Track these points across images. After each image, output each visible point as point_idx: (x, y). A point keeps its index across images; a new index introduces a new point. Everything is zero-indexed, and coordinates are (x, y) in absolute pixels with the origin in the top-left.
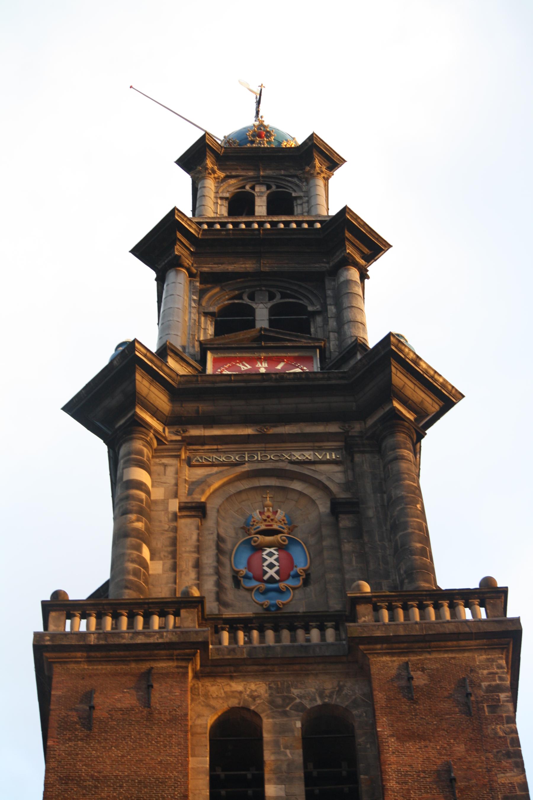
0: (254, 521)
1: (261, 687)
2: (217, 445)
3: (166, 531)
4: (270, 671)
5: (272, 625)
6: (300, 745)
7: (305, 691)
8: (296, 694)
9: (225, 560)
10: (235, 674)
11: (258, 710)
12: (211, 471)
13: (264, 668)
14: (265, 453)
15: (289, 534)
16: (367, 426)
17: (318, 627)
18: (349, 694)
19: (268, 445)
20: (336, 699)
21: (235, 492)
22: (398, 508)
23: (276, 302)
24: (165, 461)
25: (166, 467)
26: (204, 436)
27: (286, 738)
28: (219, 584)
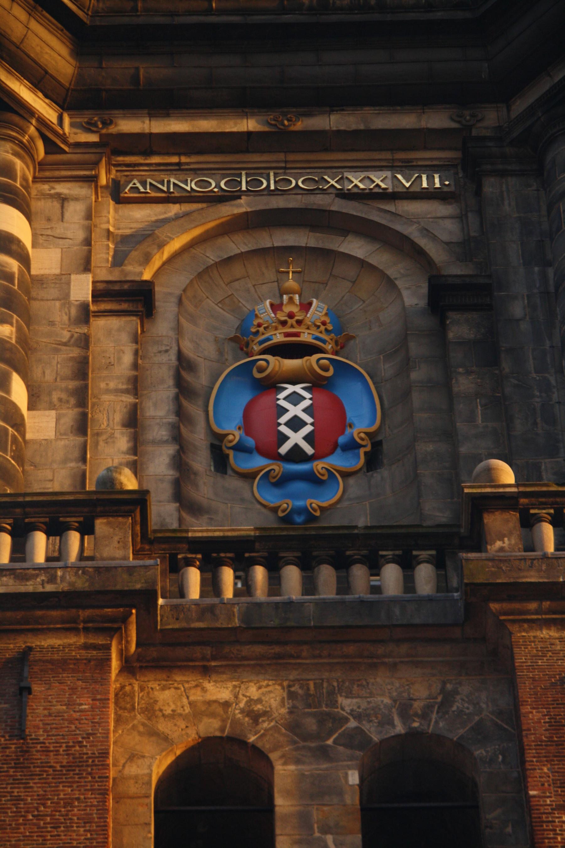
0: (259, 325)
1: (270, 692)
2: (179, 154)
3: (65, 344)
4: (291, 656)
5: (298, 554)
6: (358, 825)
7: (369, 703)
8: (348, 709)
10: (213, 664)
11: (265, 745)
12: (165, 213)
13: (277, 649)
14: (285, 174)
15: (336, 353)
16: (514, 115)
18: (467, 711)
19: (291, 157)
20: (437, 722)
21: (217, 260)
24: (62, 188)
25: (66, 204)
26: (151, 134)
27: (325, 808)
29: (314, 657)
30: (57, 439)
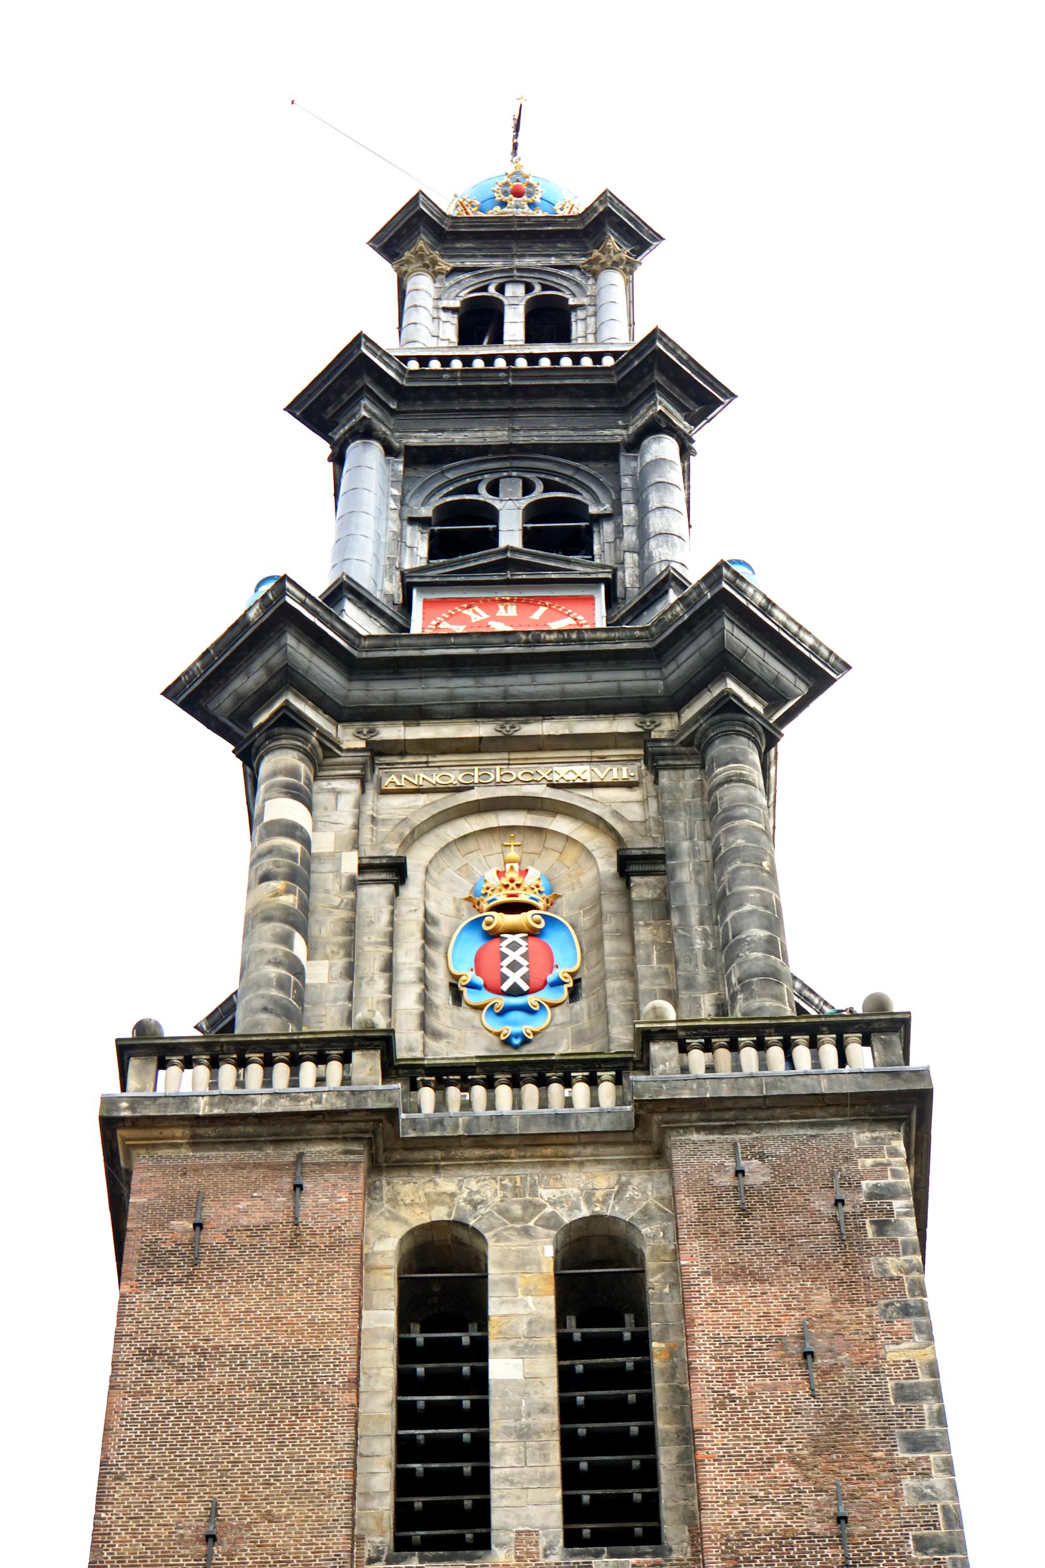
0: (488, 888)
1: (487, 1185)
2: (427, 755)
3: (337, 908)
4: (503, 1157)
5: (509, 1076)
6: (552, 1288)
7: (562, 1192)
8: (546, 1198)
9: (436, 955)
10: (443, 1163)
11: (481, 1227)
12: (416, 801)
13: (492, 1152)
14: (508, 768)
15: (547, 909)
16: (683, 722)
17: (585, 1080)
18: (637, 1198)
19: (513, 756)
20: (613, 1207)
21: (456, 837)
22: (730, 869)
23: (536, 499)
24: (337, 784)
25: (339, 796)
26: (405, 740)
27: (527, 1276)
28: (425, 1000)
29: (521, 1157)
30: (330, 983)
